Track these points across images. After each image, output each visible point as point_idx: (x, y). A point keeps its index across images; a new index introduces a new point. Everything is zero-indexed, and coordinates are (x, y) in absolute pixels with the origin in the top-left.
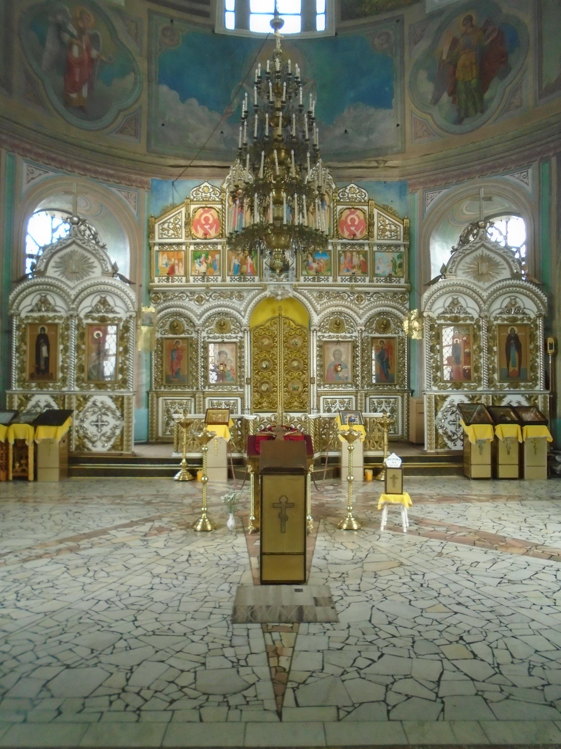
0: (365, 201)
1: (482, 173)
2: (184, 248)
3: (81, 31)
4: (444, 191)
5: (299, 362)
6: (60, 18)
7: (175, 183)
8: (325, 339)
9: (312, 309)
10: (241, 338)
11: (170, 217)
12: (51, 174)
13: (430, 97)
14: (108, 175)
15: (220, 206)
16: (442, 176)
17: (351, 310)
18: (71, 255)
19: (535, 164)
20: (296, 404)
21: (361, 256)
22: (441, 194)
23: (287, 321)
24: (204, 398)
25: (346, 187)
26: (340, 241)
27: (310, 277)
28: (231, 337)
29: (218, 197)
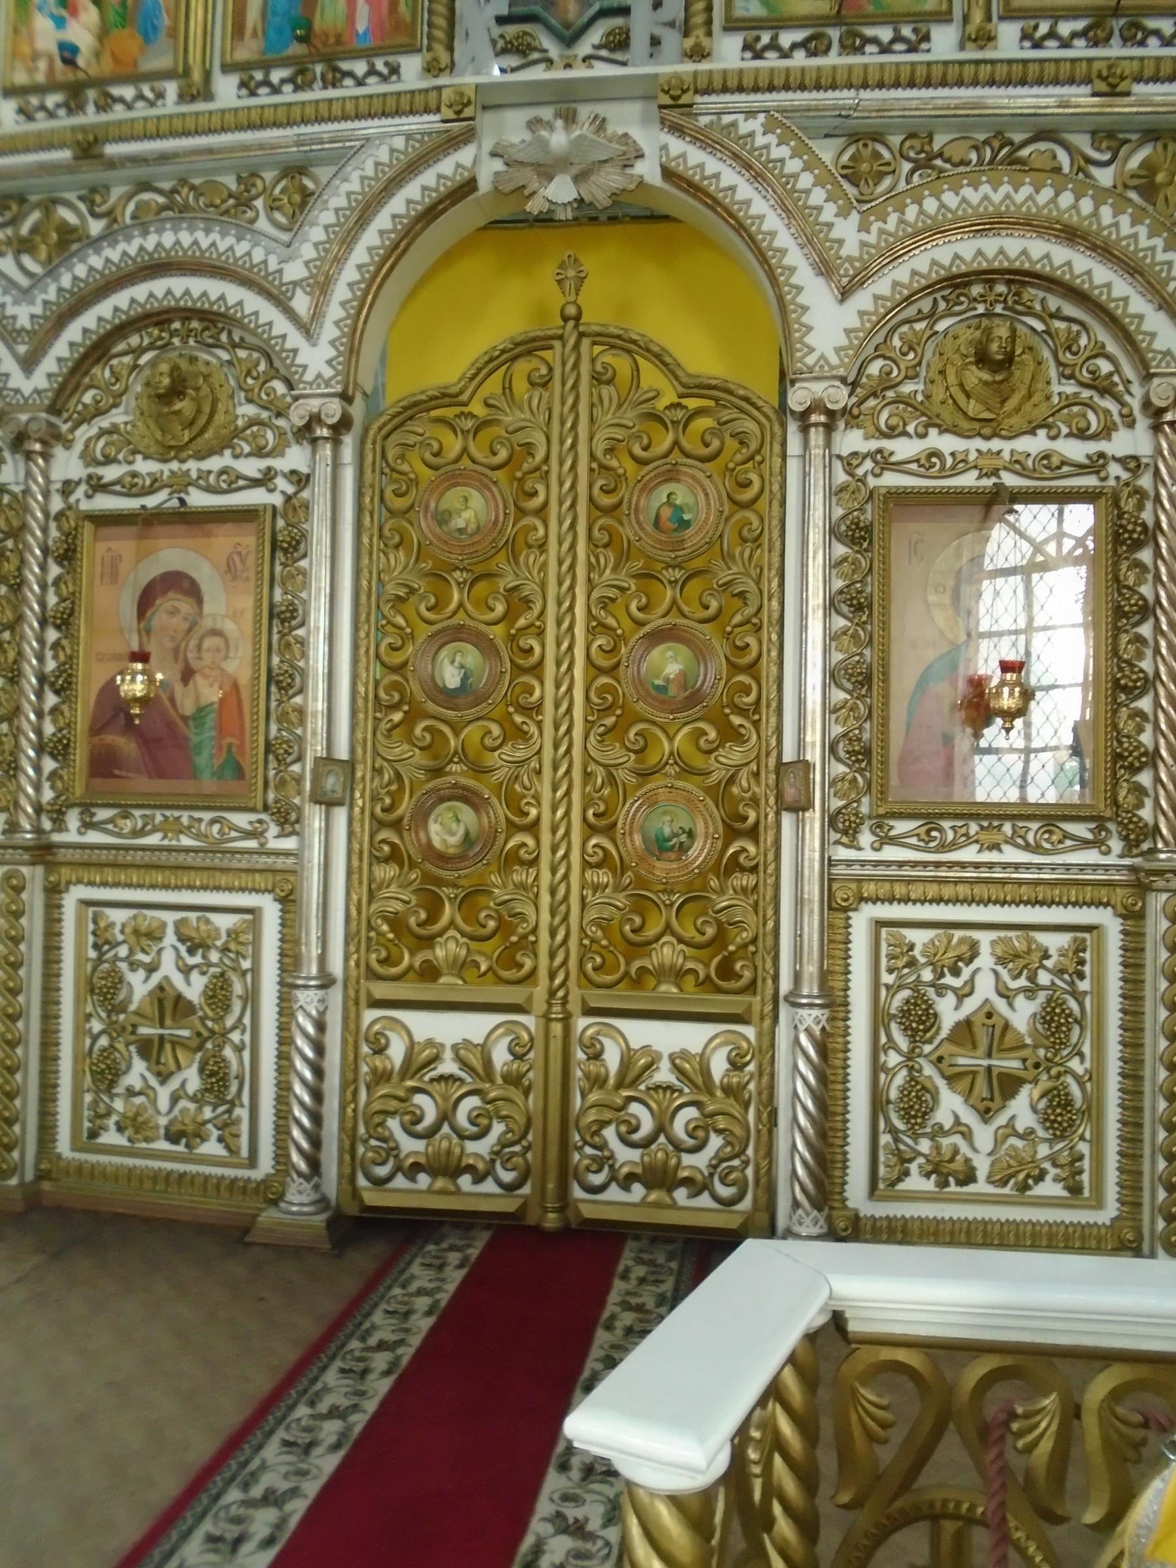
5: (700, 652)
8: (891, 480)
9: (795, 257)
10: (301, 480)
17: (1104, 250)
20: (667, 953)
23: (621, 364)
24: (54, 892)
27: (787, 39)
28: (232, 481)
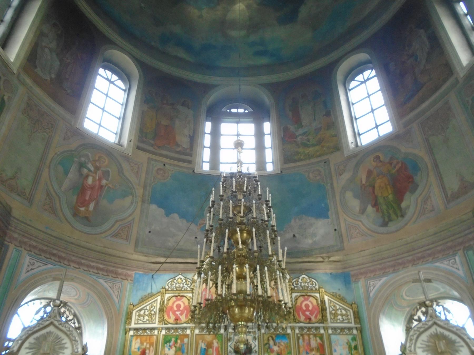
0: (316, 289)
1: (414, 262)
2: (156, 332)
3: (97, 168)
4: (384, 279)
6: (83, 159)
7: (155, 276)
11: (147, 305)
12: (50, 266)
13: (358, 209)
14: (98, 269)
15: (190, 295)
16: (379, 266)
18: (45, 337)
19: (460, 252)
21: (318, 338)
22: (382, 281)
25: (298, 278)
26: (298, 325)
29: (189, 287)
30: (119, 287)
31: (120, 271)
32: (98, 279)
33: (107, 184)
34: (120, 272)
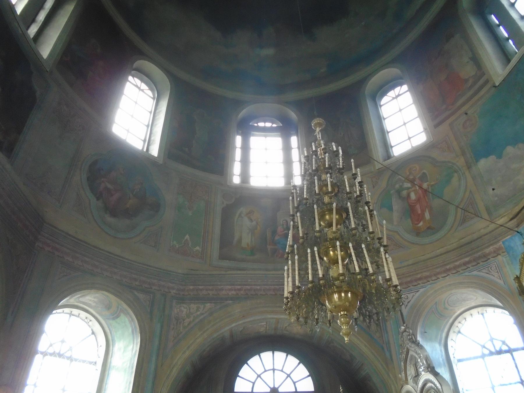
3: (412, 182)
12: (422, 290)
30: (496, 266)
31: (487, 251)
32: (472, 273)
33: (428, 185)
34: (488, 252)
